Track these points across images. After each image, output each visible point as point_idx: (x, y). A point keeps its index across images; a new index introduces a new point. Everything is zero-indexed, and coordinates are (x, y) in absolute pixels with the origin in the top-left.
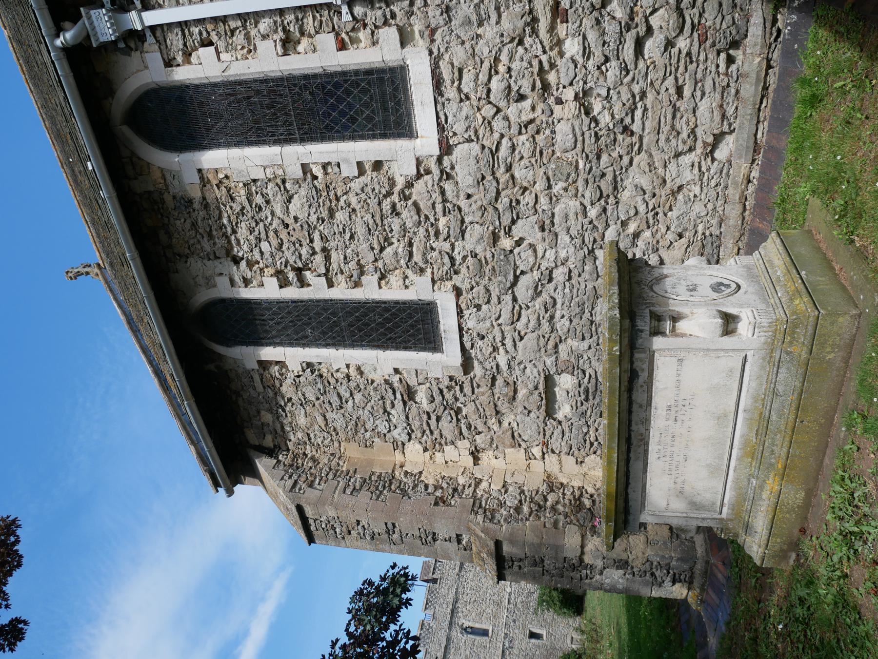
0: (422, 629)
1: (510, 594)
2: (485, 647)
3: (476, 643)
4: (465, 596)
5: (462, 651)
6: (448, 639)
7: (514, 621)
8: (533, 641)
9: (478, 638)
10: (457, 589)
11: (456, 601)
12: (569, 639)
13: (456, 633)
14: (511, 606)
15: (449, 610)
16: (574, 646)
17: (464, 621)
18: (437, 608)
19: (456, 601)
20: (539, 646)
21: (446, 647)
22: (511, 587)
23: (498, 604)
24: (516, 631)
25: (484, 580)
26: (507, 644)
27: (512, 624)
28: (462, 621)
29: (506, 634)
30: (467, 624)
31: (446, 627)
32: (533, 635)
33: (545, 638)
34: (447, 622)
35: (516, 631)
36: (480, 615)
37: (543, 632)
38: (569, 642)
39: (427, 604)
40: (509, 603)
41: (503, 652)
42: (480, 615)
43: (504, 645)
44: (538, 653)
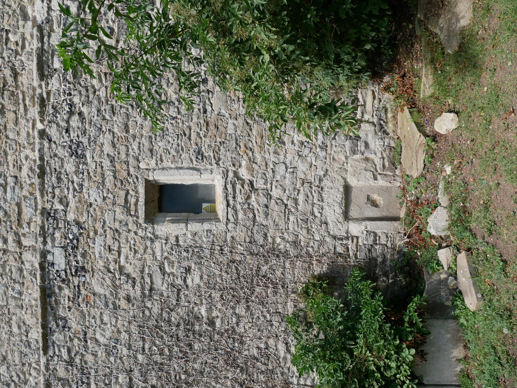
7: (77, 152)
8: (168, 228)
12: (333, 196)
14: (54, 84)
16: (355, 229)
20: (195, 250)
24: (93, 195)
26: (58, 258)
29: (46, 213)
32: (167, 201)
33: (220, 206)
37: (213, 179)
38: (332, 213)
40: (44, 71)
41: (47, 294)
44: (194, 279)
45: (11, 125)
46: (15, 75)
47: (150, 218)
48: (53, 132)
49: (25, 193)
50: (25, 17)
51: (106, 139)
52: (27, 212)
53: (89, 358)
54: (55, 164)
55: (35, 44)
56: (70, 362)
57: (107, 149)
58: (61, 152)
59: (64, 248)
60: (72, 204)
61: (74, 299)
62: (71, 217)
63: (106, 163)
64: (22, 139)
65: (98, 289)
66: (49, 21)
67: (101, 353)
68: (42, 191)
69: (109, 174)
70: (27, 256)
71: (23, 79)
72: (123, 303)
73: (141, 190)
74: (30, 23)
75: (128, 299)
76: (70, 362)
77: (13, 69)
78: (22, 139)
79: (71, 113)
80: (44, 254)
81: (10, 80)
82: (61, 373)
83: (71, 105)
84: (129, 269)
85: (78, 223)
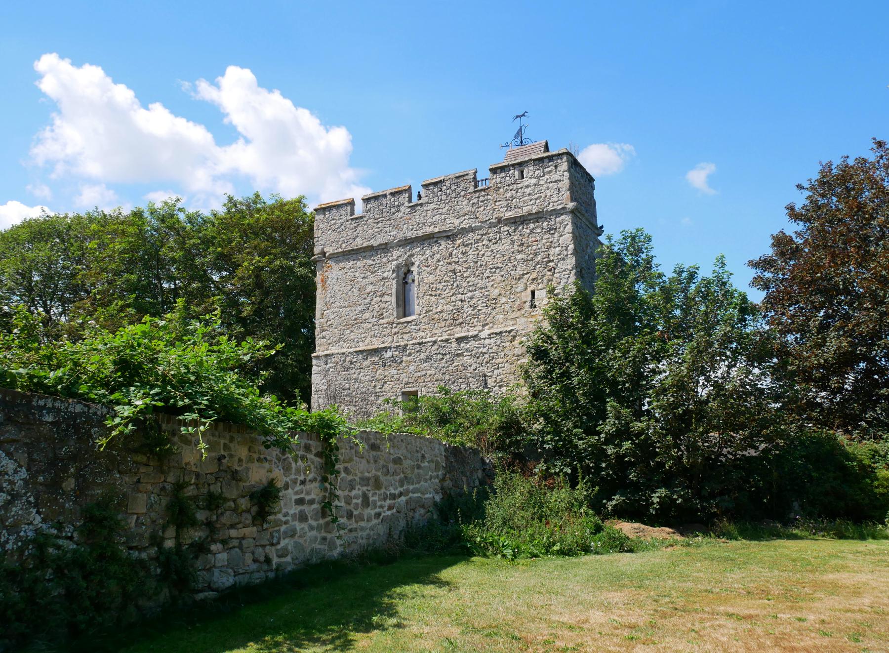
0: (393, 194)
1: (475, 337)
2: (381, 316)
3: (386, 298)
4: (462, 249)
5: (371, 278)
6: (385, 248)
7: (429, 358)
9: (394, 299)
10: (471, 230)
11: (450, 236)
13: (398, 255)
14: (454, 345)
15: (430, 230)
17: (417, 263)
18: (432, 206)
19: (450, 236)
21: (371, 248)
22: (490, 336)
23: (455, 322)
24: (412, 368)
25: (498, 277)
26: (388, 354)
27: (423, 356)
28: (417, 260)
30: (414, 269)
31: (401, 236)
34: (409, 234)
35: (412, 368)
36: (432, 291)
39: (435, 184)
40: (460, 340)
41: (375, 351)
42: (432, 291)
43: (386, 349)
45: (440, 325)
46: (460, 324)
47: (404, 393)
48: (436, 347)
49: (414, 335)
50: (484, 326)
51: (432, 372)
52: (406, 337)
53: (354, 371)
54: (424, 349)
55: (471, 334)
56: (352, 363)
57: (429, 372)
58: (428, 351)
59: (393, 356)
60: (409, 358)
61: (373, 363)
62: (404, 358)
63: (423, 373)
64: (434, 331)
65: (378, 373)
66: (480, 339)
67: (355, 376)
68: (414, 344)
69: (419, 374)
70: (390, 338)
71: (459, 328)
72: (373, 384)
73: (414, 389)
74: (481, 328)
75: (375, 386)
76: (352, 363)
77: (462, 323)
78: (434, 331)
79: (443, 354)
80: (390, 348)
81: (457, 322)
82: (348, 359)
83: (446, 354)
84: (386, 386)
85: (402, 362)
